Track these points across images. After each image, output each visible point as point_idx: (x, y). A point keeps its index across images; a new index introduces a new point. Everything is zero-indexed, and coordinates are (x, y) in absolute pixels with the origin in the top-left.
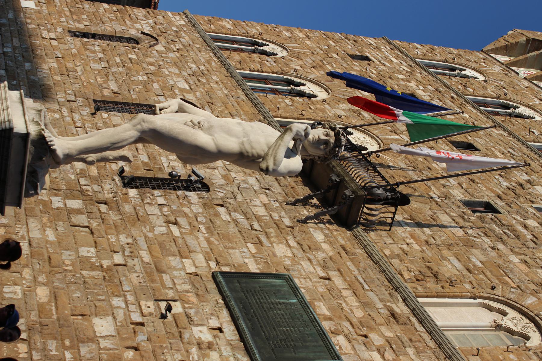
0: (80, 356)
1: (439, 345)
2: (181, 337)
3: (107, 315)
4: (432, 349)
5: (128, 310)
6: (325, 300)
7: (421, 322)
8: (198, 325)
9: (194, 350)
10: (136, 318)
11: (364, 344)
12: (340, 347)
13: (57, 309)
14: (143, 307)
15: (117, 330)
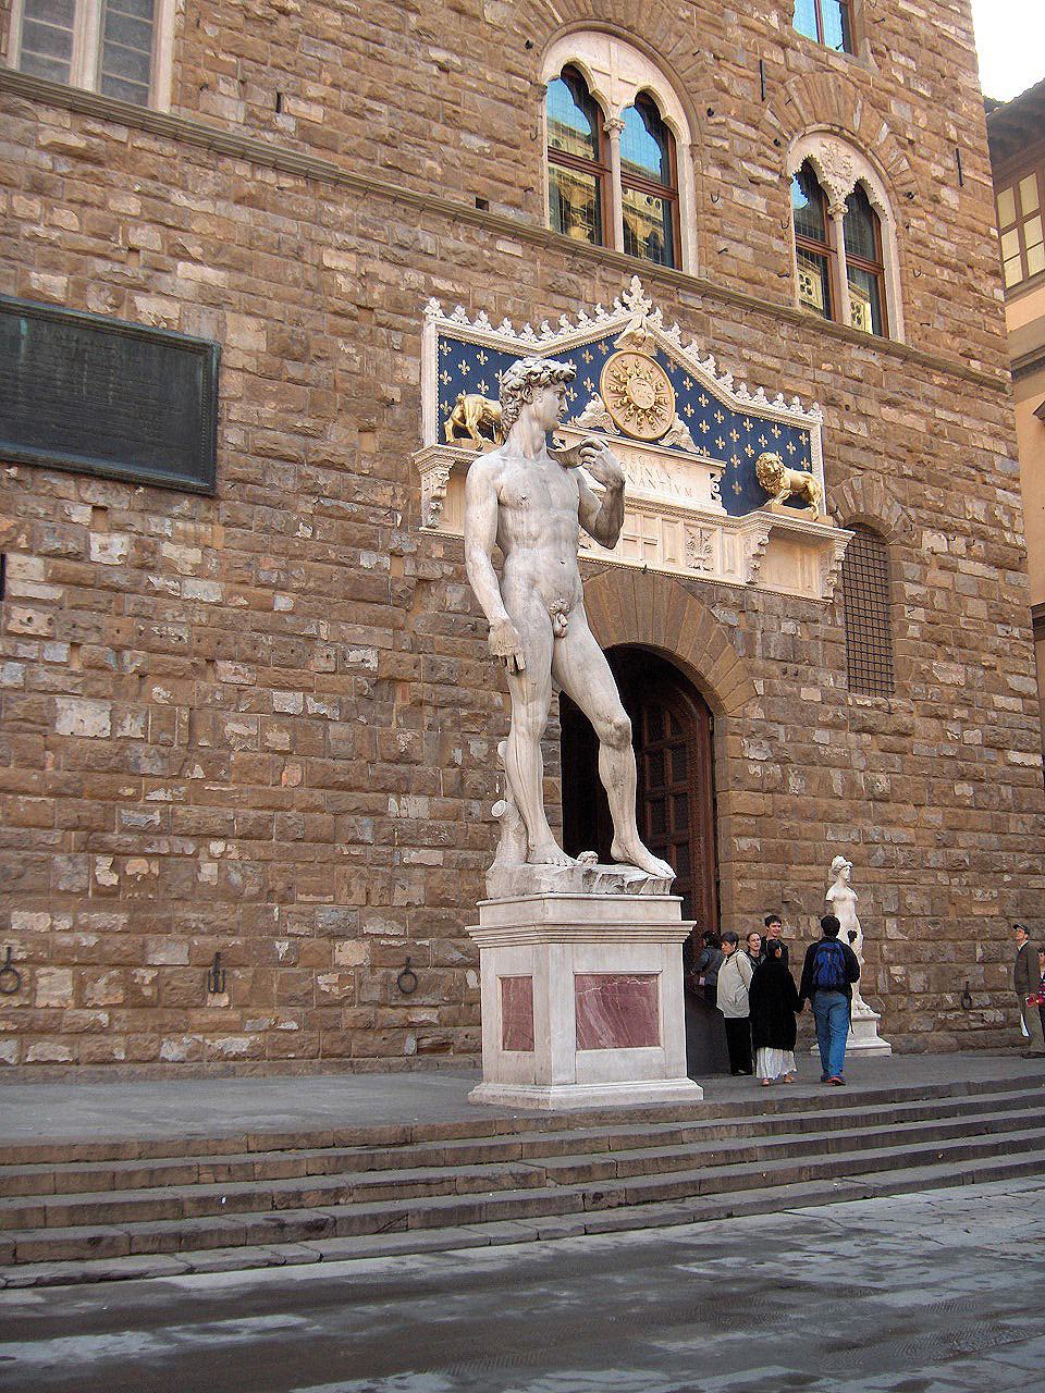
0: (159, 776)
1: (176, 139)
2: (118, 591)
3: (52, 703)
4: (175, 157)
5: (33, 661)
6: (21, 261)
7: (108, 120)
8: (89, 548)
9: (158, 582)
10: (60, 652)
11: (157, 270)
12: (166, 320)
13: (25, 792)
14: (29, 630)
15: (91, 696)
